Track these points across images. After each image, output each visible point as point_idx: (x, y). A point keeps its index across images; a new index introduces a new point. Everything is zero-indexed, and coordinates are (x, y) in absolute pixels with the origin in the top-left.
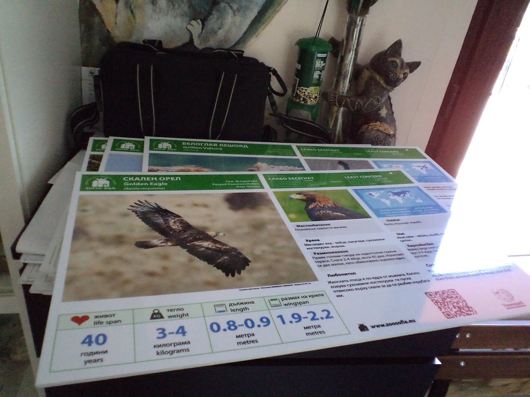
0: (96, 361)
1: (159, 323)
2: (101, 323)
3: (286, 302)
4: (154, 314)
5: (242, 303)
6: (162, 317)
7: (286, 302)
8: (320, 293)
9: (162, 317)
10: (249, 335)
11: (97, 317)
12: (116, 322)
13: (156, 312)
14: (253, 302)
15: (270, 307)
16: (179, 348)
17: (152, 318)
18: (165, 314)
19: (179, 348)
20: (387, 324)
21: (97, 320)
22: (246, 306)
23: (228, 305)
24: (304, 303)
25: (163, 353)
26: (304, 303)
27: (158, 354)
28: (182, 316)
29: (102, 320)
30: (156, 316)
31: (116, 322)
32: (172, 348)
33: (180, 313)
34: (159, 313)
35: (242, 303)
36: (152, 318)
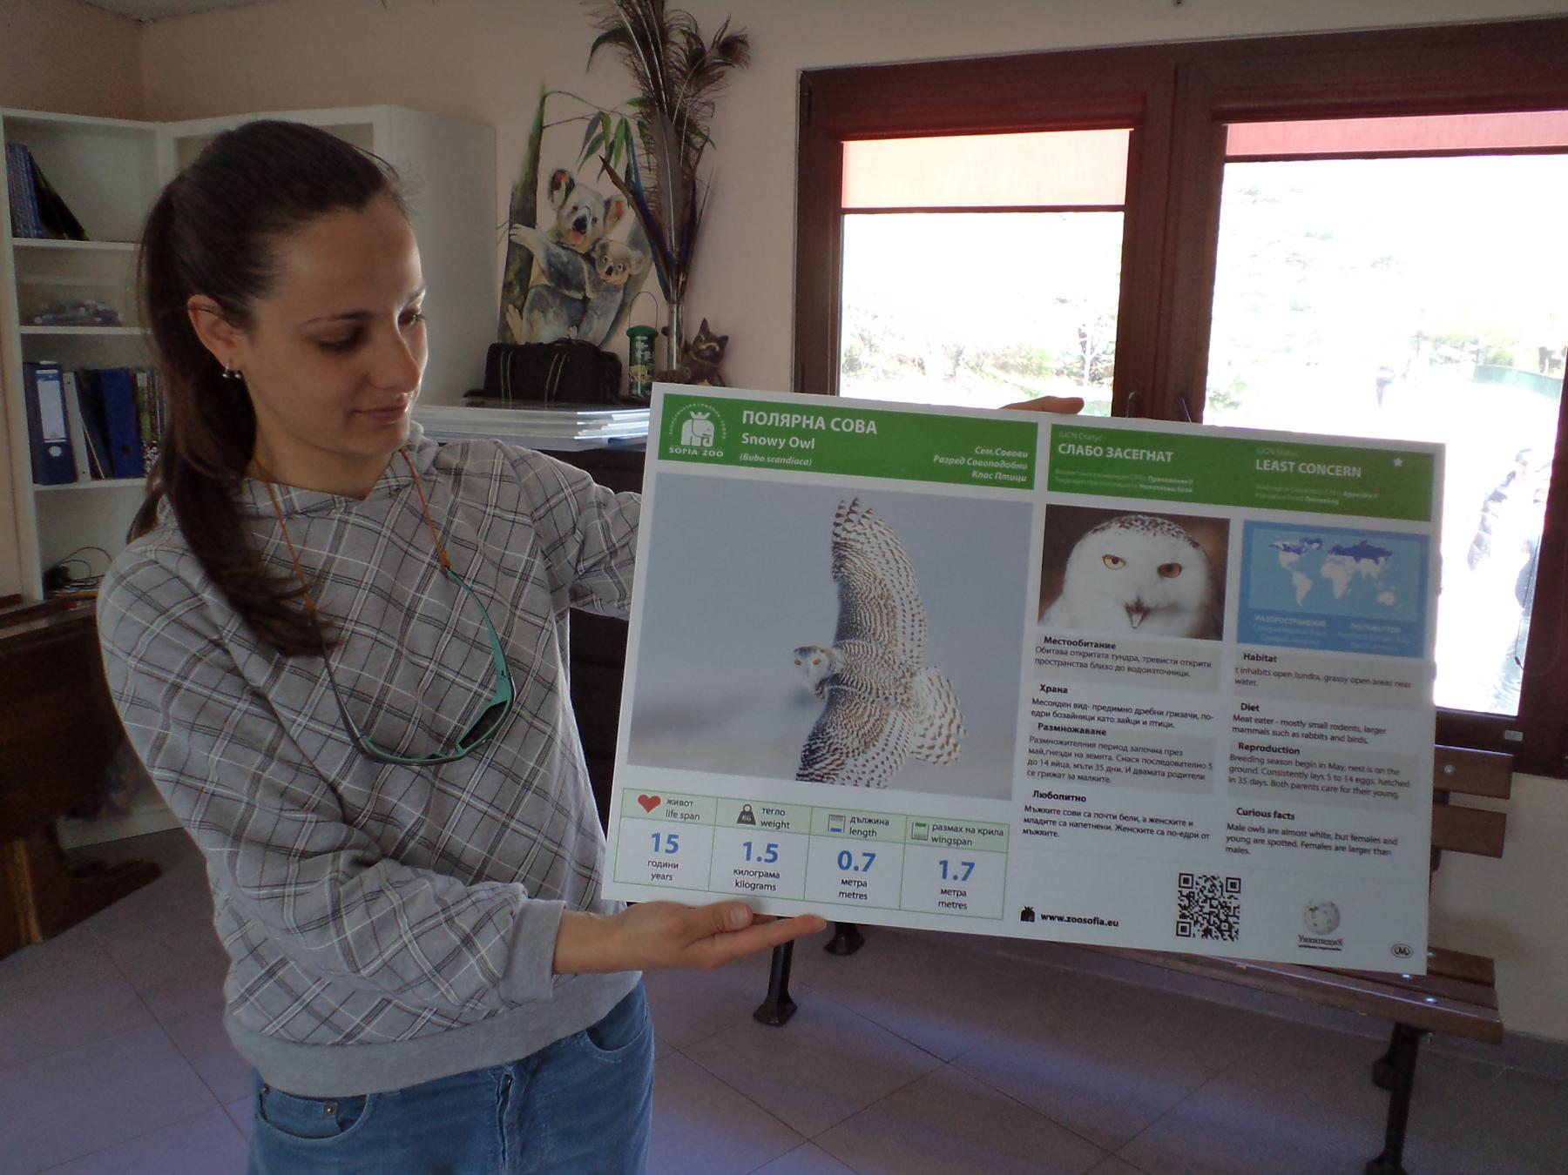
1: (747, 833)
2: (675, 815)
3: (937, 834)
4: (744, 813)
5: (870, 821)
6: (753, 822)
7: (937, 834)
8: (999, 828)
9: (753, 822)
11: (670, 802)
12: (692, 817)
13: (747, 809)
14: (887, 823)
15: (909, 840)
17: (740, 821)
18: (759, 816)
20: (1069, 918)
21: (672, 807)
23: (849, 819)
24: (965, 842)
26: (965, 842)
27: (737, 884)
28: (779, 826)
30: (747, 817)
31: (692, 817)
33: (778, 819)
34: (750, 814)
35: (870, 821)
36: (740, 821)
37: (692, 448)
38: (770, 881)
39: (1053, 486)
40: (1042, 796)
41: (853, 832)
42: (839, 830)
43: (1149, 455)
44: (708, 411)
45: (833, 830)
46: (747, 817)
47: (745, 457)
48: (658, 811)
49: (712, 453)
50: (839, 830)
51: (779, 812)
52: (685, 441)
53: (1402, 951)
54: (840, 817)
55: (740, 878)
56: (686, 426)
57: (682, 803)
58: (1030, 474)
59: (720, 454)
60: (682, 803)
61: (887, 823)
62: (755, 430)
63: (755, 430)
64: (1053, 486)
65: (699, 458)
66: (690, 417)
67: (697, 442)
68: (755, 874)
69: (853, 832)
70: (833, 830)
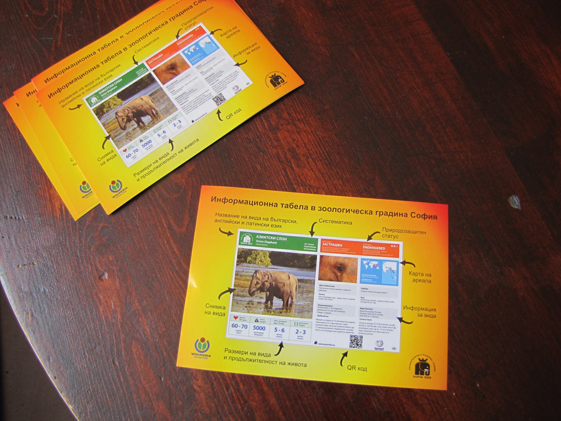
0: (239, 333)
4: (256, 320)
6: (258, 322)
9: (258, 322)
10: (280, 335)
11: (240, 317)
14: (286, 322)
16: (260, 334)
17: (255, 321)
18: (259, 321)
19: (260, 334)
21: (240, 318)
22: (284, 323)
25: (256, 335)
28: (263, 322)
29: (241, 319)
30: (257, 321)
32: (258, 334)
33: (263, 321)
34: (257, 320)
36: (255, 321)
37: (246, 243)
38: (262, 334)
39: (321, 251)
40: (319, 316)
41: (279, 323)
42: (276, 323)
43: (340, 245)
44: (249, 235)
45: (275, 323)
46: (257, 321)
47: (257, 244)
48: (238, 319)
49: (250, 244)
50: (276, 323)
51: (264, 320)
52: (244, 241)
53: (394, 349)
54: (277, 321)
55: (255, 333)
56: (245, 238)
57: (243, 318)
58: (317, 249)
59: (252, 244)
60: (243, 318)
61: (286, 322)
62: (259, 239)
63: (259, 239)
64: (321, 251)
65: (247, 245)
66: (245, 236)
67: (247, 242)
68: (258, 333)
69: (279, 323)
70: (275, 323)
